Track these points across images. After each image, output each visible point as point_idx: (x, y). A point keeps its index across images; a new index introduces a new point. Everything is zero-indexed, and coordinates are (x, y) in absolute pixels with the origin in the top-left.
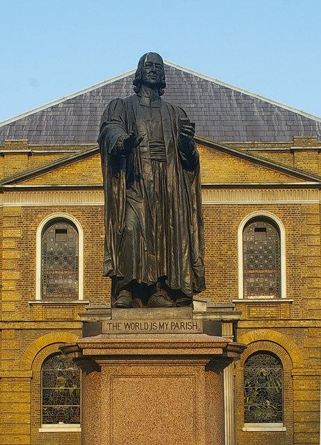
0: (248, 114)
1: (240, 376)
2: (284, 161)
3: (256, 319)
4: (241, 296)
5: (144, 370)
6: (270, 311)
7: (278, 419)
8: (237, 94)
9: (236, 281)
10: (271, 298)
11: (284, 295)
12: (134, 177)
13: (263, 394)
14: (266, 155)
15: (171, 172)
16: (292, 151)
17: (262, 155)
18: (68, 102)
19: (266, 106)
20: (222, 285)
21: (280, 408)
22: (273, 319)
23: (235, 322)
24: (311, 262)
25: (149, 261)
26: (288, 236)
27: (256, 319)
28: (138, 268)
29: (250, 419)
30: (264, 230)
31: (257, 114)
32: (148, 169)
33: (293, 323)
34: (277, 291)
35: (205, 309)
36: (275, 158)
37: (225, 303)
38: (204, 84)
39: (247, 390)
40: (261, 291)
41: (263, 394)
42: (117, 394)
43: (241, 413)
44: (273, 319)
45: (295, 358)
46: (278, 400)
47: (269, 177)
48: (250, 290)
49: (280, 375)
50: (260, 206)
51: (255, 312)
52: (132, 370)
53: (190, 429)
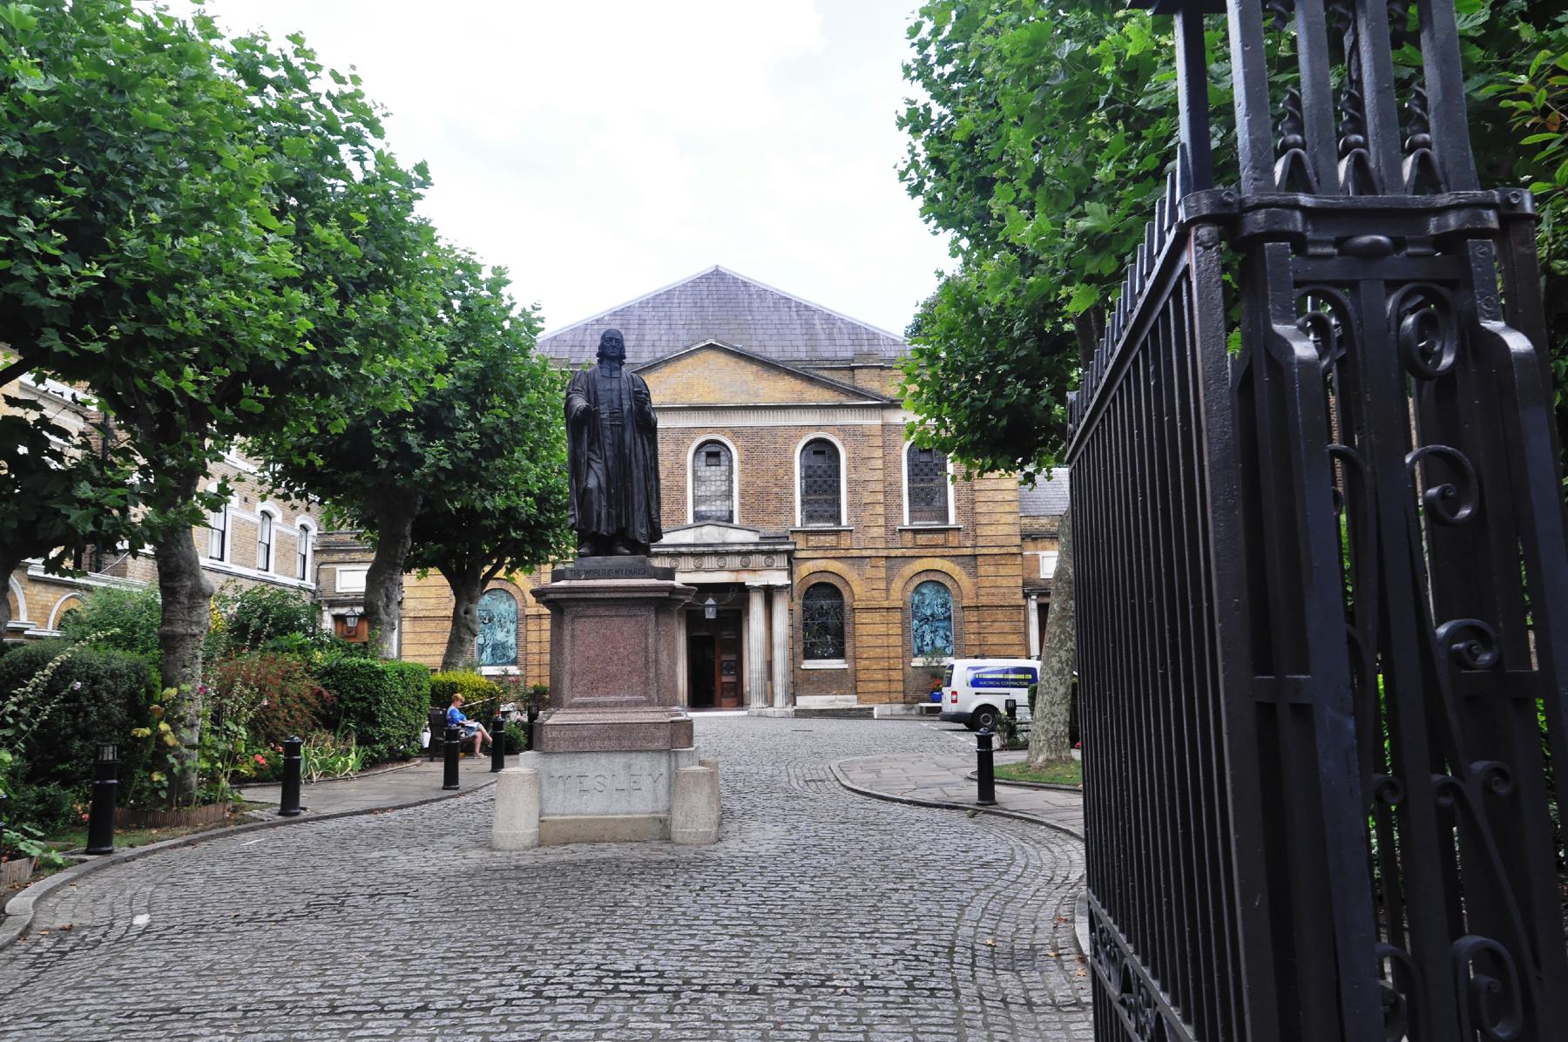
0: (809, 325)
1: (798, 609)
2: (842, 378)
3: (816, 548)
4: (798, 524)
5: (601, 611)
6: (830, 540)
7: (840, 654)
8: (799, 304)
9: (793, 509)
10: (829, 526)
11: (844, 521)
12: (595, 438)
13: (824, 629)
14: (825, 374)
15: (628, 437)
16: (852, 369)
17: (821, 373)
18: (615, 314)
19: (829, 319)
20: (778, 512)
21: (843, 644)
22: (832, 548)
23: (790, 554)
24: (872, 486)
25: (608, 513)
26: (848, 459)
27: (816, 548)
28: (599, 522)
29: (809, 655)
30: (823, 453)
31: (818, 327)
32: (608, 433)
33: (855, 553)
34: (836, 518)
35: (757, 539)
36: (837, 377)
37: (781, 531)
38: (763, 293)
39: (806, 625)
40: (821, 518)
41: (824, 629)
42: (578, 632)
43: (799, 649)
44: (832, 548)
45: (857, 590)
46: (840, 635)
47: (828, 397)
48: (809, 517)
49: (841, 606)
50: (819, 427)
51: (814, 541)
52: (590, 612)
53: (641, 662)
